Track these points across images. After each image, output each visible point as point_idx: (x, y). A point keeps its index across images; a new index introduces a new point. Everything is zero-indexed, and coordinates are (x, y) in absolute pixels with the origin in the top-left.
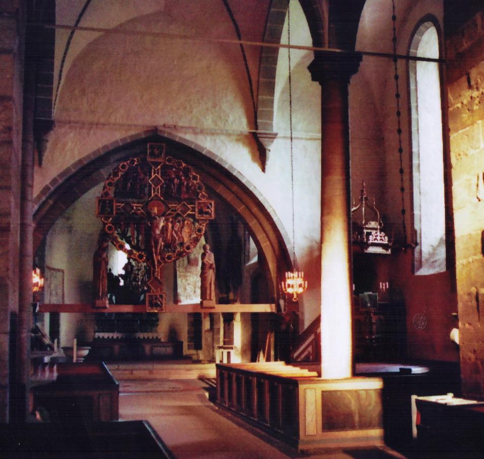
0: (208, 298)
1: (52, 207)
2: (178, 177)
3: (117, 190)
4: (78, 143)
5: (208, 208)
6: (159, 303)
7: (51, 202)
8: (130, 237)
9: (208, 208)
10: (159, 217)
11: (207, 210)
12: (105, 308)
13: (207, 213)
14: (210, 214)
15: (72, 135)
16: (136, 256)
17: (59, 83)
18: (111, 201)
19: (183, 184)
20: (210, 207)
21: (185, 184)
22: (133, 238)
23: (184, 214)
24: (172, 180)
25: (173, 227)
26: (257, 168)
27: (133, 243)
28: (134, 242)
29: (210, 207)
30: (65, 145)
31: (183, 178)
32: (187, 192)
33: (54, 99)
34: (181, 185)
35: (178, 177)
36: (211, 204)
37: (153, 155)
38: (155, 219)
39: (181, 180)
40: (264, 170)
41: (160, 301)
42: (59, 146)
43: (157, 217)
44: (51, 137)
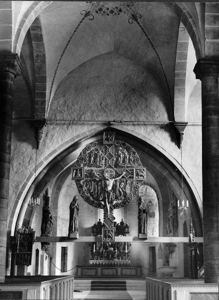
0: (142, 232)
1: (46, 175)
2: (123, 153)
5: (142, 172)
7: (45, 171)
9: (142, 172)
11: (141, 174)
12: (76, 238)
13: (141, 176)
14: (144, 177)
15: (57, 129)
17: (50, 98)
18: (81, 170)
19: (126, 157)
24: (120, 156)
25: (119, 185)
26: (173, 145)
31: (126, 154)
32: (129, 162)
33: (46, 107)
34: (125, 158)
35: (123, 153)
36: (144, 170)
37: (107, 139)
39: (125, 154)
40: (179, 146)
44: (45, 129)
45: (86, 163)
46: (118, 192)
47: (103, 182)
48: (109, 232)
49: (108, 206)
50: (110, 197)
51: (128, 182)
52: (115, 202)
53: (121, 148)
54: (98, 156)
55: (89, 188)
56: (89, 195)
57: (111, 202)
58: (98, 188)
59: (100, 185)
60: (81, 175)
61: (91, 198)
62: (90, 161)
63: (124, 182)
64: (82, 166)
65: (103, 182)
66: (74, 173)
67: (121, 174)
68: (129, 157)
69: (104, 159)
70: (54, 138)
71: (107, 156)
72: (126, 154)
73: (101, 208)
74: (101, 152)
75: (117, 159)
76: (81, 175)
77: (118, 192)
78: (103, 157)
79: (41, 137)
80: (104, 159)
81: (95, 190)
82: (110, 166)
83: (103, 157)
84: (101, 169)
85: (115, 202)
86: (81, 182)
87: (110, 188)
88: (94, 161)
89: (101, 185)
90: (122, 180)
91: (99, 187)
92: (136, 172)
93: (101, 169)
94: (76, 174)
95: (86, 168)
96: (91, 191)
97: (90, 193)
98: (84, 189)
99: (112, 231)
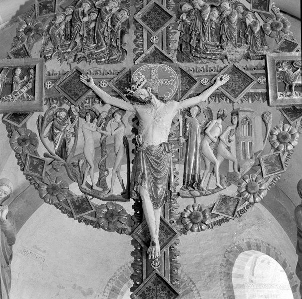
23: (236, 97)
49: (153, 216)
51: (242, 115)
52: (182, 204)
54: (107, 18)
55: (64, 145)
57: (166, 201)
63: (222, 116)
68: (242, 22)
69: (132, 26)
71: (144, 19)
73: (121, 231)
80: (132, 26)
82: (159, 56)
84: (117, 67)
85: (182, 204)
86: (31, 123)
90: (215, 107)
93: (117, 67)
95: (54, 66)
98: (41, 151)
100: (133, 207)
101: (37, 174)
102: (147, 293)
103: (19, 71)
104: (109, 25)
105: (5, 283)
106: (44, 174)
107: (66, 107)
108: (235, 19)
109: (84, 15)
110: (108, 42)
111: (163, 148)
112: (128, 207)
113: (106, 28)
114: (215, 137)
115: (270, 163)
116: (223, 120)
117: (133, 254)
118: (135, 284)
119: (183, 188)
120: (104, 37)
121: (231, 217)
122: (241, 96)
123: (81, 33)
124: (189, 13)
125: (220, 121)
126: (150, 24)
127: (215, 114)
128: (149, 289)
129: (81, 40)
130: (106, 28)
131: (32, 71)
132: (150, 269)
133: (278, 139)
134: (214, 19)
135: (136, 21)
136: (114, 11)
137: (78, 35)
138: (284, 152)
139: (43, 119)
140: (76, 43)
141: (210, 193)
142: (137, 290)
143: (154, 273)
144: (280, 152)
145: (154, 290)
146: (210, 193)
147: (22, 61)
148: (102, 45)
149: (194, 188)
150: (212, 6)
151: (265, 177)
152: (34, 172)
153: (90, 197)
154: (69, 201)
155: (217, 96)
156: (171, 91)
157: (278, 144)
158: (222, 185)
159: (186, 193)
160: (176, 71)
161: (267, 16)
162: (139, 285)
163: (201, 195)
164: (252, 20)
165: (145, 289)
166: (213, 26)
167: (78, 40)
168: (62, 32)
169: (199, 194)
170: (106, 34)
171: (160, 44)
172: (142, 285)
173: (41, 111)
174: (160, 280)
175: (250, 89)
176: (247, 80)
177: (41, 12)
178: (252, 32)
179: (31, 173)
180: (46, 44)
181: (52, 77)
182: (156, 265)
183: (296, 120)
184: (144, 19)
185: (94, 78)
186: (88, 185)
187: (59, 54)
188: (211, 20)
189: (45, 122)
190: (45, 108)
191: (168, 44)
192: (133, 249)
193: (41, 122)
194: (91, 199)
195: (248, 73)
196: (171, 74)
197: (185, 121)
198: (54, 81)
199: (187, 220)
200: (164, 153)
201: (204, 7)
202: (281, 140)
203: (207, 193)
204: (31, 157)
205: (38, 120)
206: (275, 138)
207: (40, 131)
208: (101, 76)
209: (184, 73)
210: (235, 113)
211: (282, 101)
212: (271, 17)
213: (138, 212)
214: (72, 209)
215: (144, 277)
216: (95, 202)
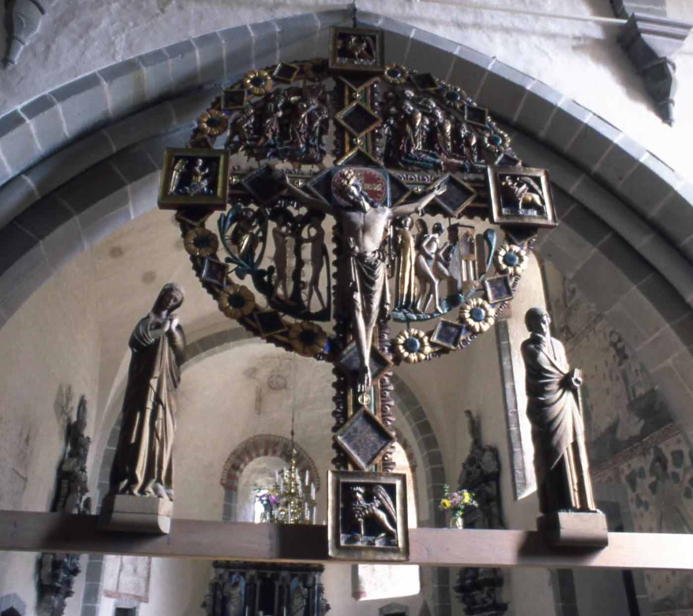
3: (236, 138)
4: (131, 24)
6: (382, 515)
8: (271, 269)
9: (532, 190)
10: (372, 205)
14: (541, 211)
16: (293, 335)
18: (211, 162)
19: (442, 127)
20: (536, 187)
21: (448, 128)
22: (282, 277)
24: (411, 119)
25: (418, 247)
27: (280, 291)
28: (284, 289)
29: (536, 187)
30: (89, 26)
31: (439, 114)
32: (457, 150)
36: (537, 180)
38: (358, 208)
39: (432, 116)
41: (382, 508)
42: (73, 24)
43: (367, 206)
45: (242, 140)
46: (409, 277)
47: (329, 222)
48: (369, 497)
50: (379, 282)
53: (410, 93)
56: (248, 282)
58: (298, 251)
59: (310, 239)
60: (213, 185)
61: (261, 300)
62: (259, 129)
63: (438, 229)
64: (219, 144)
65: (329, 222)
66: (175, 175)
67: (424, 194)
68: (455, 132)
70: (93, 33)
72: (439, 114)
74: (314, 104)
75: (398, 134)
76: (213, 185)
77: (409, 277)
78: (325, 122)
79: (32, 27)
80: (332, 128)
81: (280, 257)
83: (325, 122)
86: (212, 223)
87: (371, 244)
88: (284, 134)
89: (318, 241)
90: (431, 220)
91: (307, 251)
92: (498, 187)
94: (186, 179)
96: (265, 265)
97: (258, 277)
98: (222, 255)
99: (391, 489)
100: (335, 328)
101: (216, 282)
102: (354, 434)
103: (200, 162)
104: (306, 121)
105: (171, 411)
106: (225, 282)
107: (254, 207)
108: (448, 128)
109: (276, 110)
110: (304, 140)
111: (377, 255)
112: (328, 327)
113: (303, 125)
114: (432, 253)
115: (496, 287)
116: (439, 235)
117: (335, 385)
118: (338, 422)
119: (396, 309)
120: (300, 134)
121: (453, 347)
122: (460, 211)
123: (273, 128)
124: (396, 117)
125: (436, 236)
126: (352, 125)
127: (430, 230)
128: (355, 430)
129: (274, 136)
130: (303, 125)
131: (214, 164)
132: (357, 406)
133: (505, 261)
134: (425, 127)
135: (336, 123)
136: (313, 107)
137: (270, 130)
138: (511, 276)
139: (226, 218)
140: (267, 138)
141: (429, 317)
142: (341, 431)
143: (362, 410)
144: (508, 276)
145: (361, 432)
146: (429, 317)
147: (205, 153)
148: (298, 141)
149: (409, 311)
150: (424, 114)
151: (491, 302)
152: (213, 278)
153: (281, 314)
154: (255, 316)
155: (433, 208)
156: (379, 198)
157: (504, 267)
158: (443, 310)
159: (401, 315)
160: (386, 177)
161: (483, 129)
162: (343, 424)
163: (419, 319)
164: (466, 131)
165: (351, 430)
166: (424, 134)
167: (270, 135)
168: (251, 126)
169: (415, 318)
170: (302, 130)
171: (365, 146)
172: (348, 424)
173: (223, 207)
174: (368, 418)
175: (468, 203)
176: (468, 193)
177: (226, 105)
178: (468, 144)
179: (209, 279)
180: (231, 137)
181: (237, 172)
182: (366, 400)
183: (523, 242)
184: (346, 119)
185: (289, 177)
186: (277, 298)
187: (247, 148)
188: (422, 128)
189: (228, 223)
190: (229, 207)
191: (374, 149)
192: (335, 379)
193: (222, 224)
194: (283, 316)
195: (466, 185)
196: (379, 179)
197: (396, 233)
198: (241, 176)
199: (401, 347)
200: (379, 261)
201: (413, 112)
202: (508, 261)
203: (426, 317)
204: (210, 261)
205: (219, 222)
206: (500, 259)
207: (222, 230)
208: (296, 176)
209: (394, 181)
210: (453, 229)
211: (507, 217)
212: (488, 131)
213: (341, 335)
214: (259, 326)
215: (351, 413)
216: (288, 319)
